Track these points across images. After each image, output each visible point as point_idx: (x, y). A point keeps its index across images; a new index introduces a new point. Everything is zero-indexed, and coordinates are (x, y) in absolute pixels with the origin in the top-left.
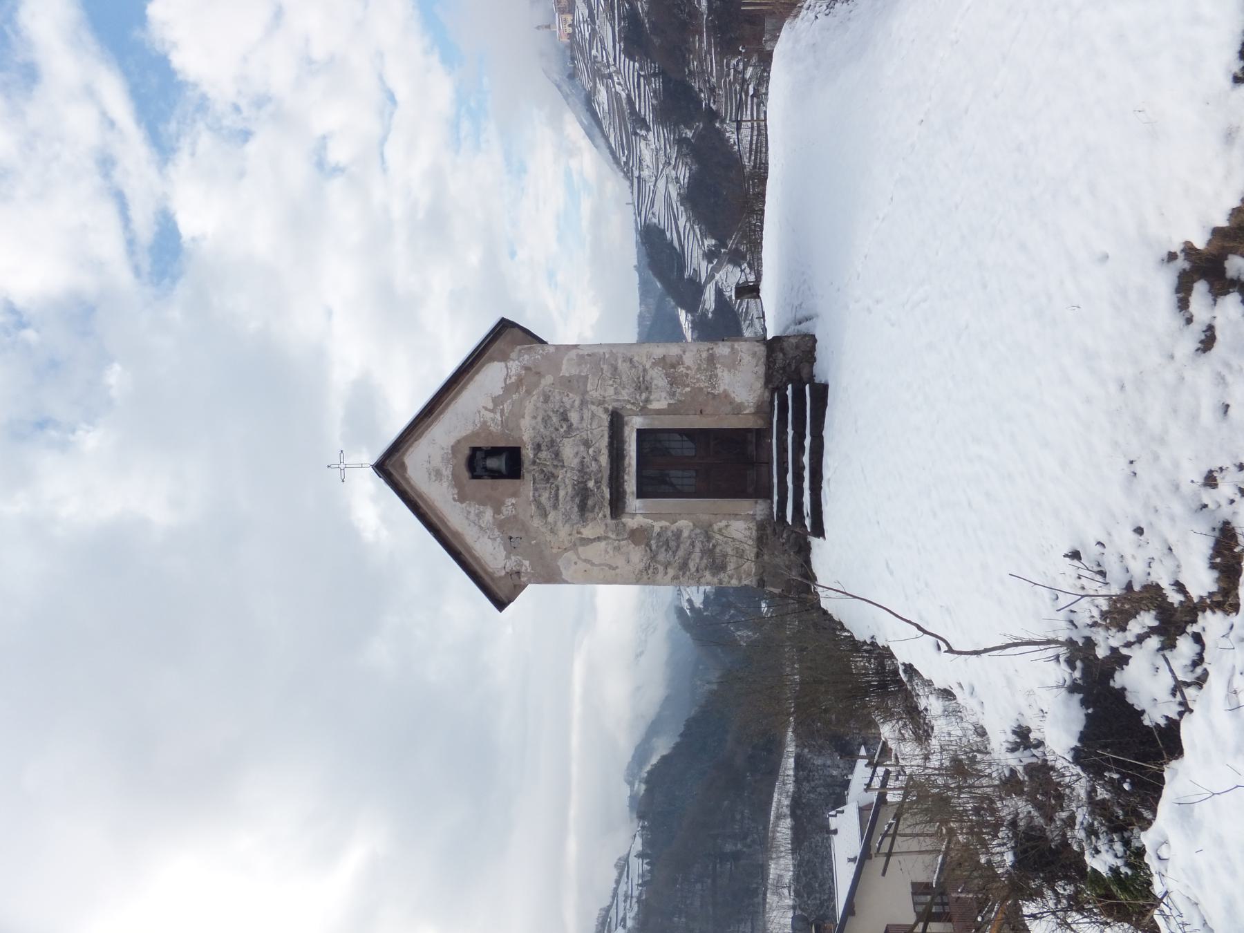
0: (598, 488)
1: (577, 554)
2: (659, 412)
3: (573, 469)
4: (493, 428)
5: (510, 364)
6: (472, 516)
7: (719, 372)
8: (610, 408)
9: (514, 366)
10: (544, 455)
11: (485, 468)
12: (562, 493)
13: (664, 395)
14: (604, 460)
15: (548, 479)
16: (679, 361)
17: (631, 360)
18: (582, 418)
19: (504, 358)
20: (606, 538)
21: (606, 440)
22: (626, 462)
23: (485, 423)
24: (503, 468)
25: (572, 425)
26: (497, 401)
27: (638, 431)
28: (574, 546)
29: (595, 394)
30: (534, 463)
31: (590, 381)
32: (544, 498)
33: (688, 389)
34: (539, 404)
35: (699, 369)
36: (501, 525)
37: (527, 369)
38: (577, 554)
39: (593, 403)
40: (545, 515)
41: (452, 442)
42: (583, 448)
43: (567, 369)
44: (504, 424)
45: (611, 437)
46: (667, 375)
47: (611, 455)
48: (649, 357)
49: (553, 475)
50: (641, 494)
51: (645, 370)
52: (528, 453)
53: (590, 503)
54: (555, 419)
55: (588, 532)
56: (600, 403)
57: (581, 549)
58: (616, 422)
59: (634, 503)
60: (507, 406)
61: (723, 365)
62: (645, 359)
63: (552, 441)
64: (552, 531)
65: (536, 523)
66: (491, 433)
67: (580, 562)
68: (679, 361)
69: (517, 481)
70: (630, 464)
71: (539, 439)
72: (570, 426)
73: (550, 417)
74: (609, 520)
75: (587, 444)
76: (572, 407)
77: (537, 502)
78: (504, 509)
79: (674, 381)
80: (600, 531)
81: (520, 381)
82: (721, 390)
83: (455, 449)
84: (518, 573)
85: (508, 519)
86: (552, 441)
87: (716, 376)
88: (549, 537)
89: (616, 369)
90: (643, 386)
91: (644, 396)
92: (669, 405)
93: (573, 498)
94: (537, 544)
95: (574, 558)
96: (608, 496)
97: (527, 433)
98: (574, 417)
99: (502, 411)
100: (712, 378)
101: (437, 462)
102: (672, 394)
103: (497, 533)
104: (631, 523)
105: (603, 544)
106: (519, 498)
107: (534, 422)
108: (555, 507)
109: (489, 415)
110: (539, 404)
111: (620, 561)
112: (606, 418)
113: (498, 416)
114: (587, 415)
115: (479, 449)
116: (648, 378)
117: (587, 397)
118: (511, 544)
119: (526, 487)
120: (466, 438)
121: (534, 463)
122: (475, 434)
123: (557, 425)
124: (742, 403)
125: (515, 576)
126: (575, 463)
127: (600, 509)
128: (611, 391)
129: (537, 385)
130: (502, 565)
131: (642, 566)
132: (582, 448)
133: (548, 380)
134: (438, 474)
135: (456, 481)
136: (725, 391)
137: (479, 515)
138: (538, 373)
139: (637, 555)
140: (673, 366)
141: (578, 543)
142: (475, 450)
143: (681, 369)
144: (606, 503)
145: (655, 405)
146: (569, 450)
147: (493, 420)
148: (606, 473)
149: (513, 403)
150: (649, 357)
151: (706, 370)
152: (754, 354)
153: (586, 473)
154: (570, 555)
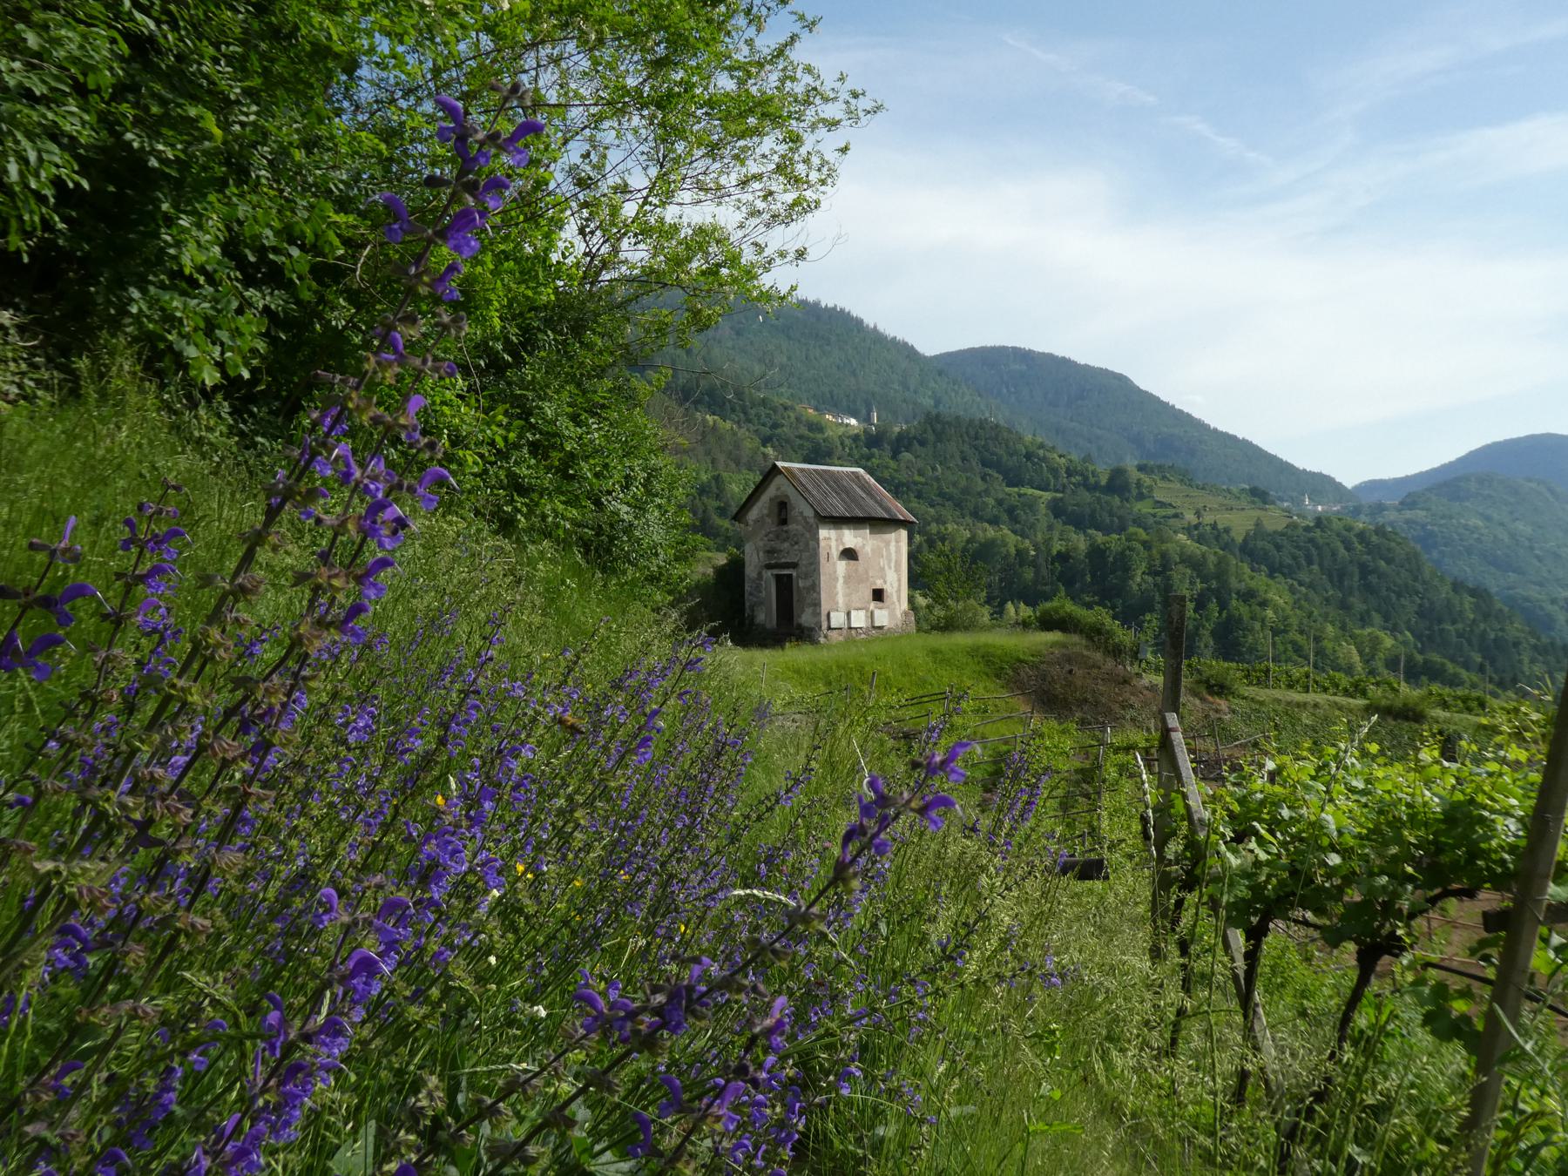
42: (789, 553)
43: (812, 543)
50: (778, 578)
58: (794, 566)
59: (768, 574)
90: (806, 576)
97: (792, 527)
106: (771, 525)
118: (757, 521)
146: (786, 545)
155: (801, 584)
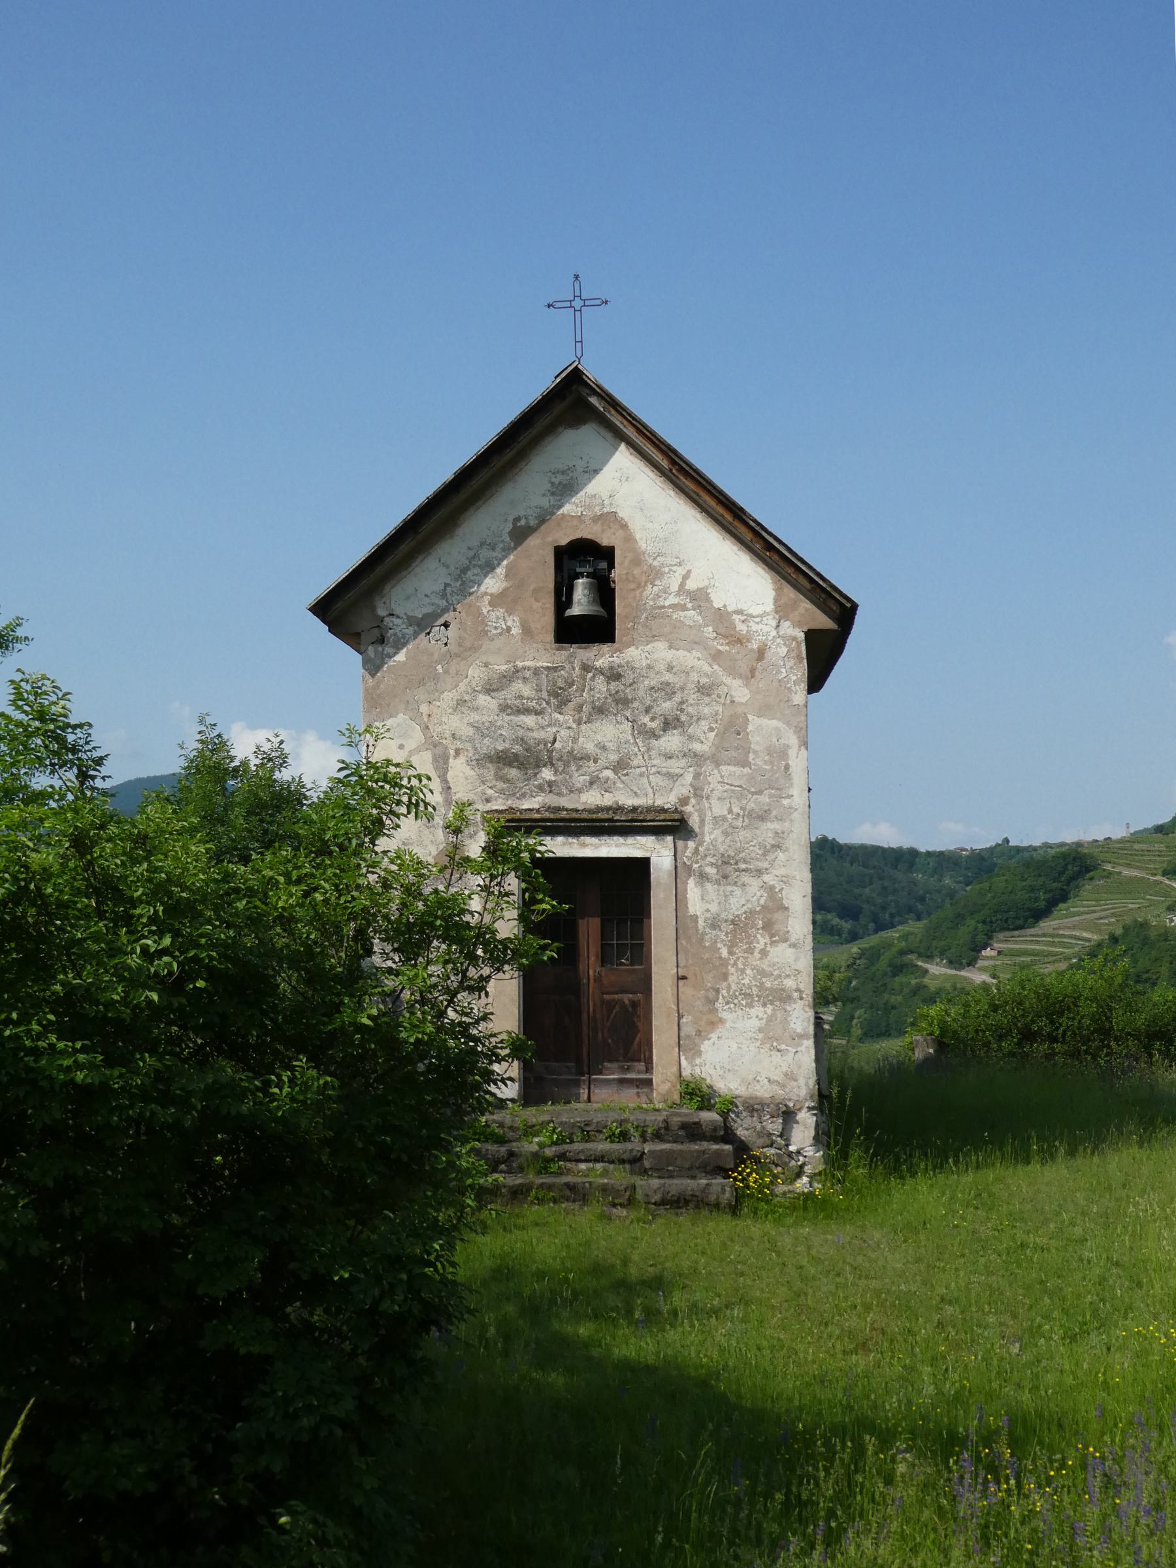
0: (541, 788)
1: (417, 750)
2: (679, 900)
3: (575, 740)
7: (758, 1010)
8: (688, 809)
10: (601, 685)
11: (578, 576)
12: (529, 720)
13: (714, 908)
14: (592, 799)
15: (556, 695)
16: (776, 935)
17: (777, 846)
19: (782, 611)
21: (628, 801)
22: (588, 840)
23: (655, 574)
24: (576, 610)
25: (657, 737)
26: (700, 598)
27: (645, 862)
29: (714, 778)
30: (586, 668)
31: (738, 770)
33: (724, 953)
34: (694, 677)
35: (763, 973)
37: (761, 654)
38: (417, 750)
39: (697, 776)
40: (489, 690)
44: (658, 614)
45: (634, 809)
46: (751, 914)
48: (786, 880)
51: (759, 872)
52: (602, 656)
53: (513, 773)
54: (666, 706)
56: (697, 791)
61: (770, 1019)
62: (782, 871)
63: (624, 702)
64: (461, 702)
65: (476, 674)
68: (776, 935)
69: (550, 637)
70: (584, 845)
71: (629, 677)
72: (653, 735)
75: (621, 766)
77: (514, 674)
78: (500, 612)
79: (740, 927)
81: (739, 640)
83: (610, 519)
84: (382, 640)
86: (624, 702)
87: (750, 1005)
88: (449, 697)
89: (762, 818)
90: (729, 868)
91: (710, 870)
92: (695, 918)
94: (436, 678)
96: (526, 805)
98: (672, 741)
99: (683, 608)
100: (747, 998)
102: (714, 925)
107: (661, 667)
108: (504, 708)
109: (675, 587)
110: (694, 677)
112: (668, 800)
113: (672, 600)
114: (675, 766)
115: (611, 566)
116: (745, 878)
117: (708, 767)
119: (543, 654)
120: (629, 539)
121: (586, 668)
122: (637, 559)
123: (657, 710)
124: (699, 1053)
125: (376, 632)
126: (588, 746)
127: (502, 792)
128: (719, 809)
129: (732, 672)
130: (398, 610)
132: (614, 757)
133: (741, 692)
136: (721, 1021)
138: (753, 671)
140: (768, 926)
141: (439, 750)
142: (607, 554)
143: (762, 941)
145: (693, 890)
146: (608, 733)
147: (666, 591)
148: (567, 802)
150: (786, 880)
151: (761, 987)
152: (790, 1076)
153: (567, 764)
155: (697, 900)
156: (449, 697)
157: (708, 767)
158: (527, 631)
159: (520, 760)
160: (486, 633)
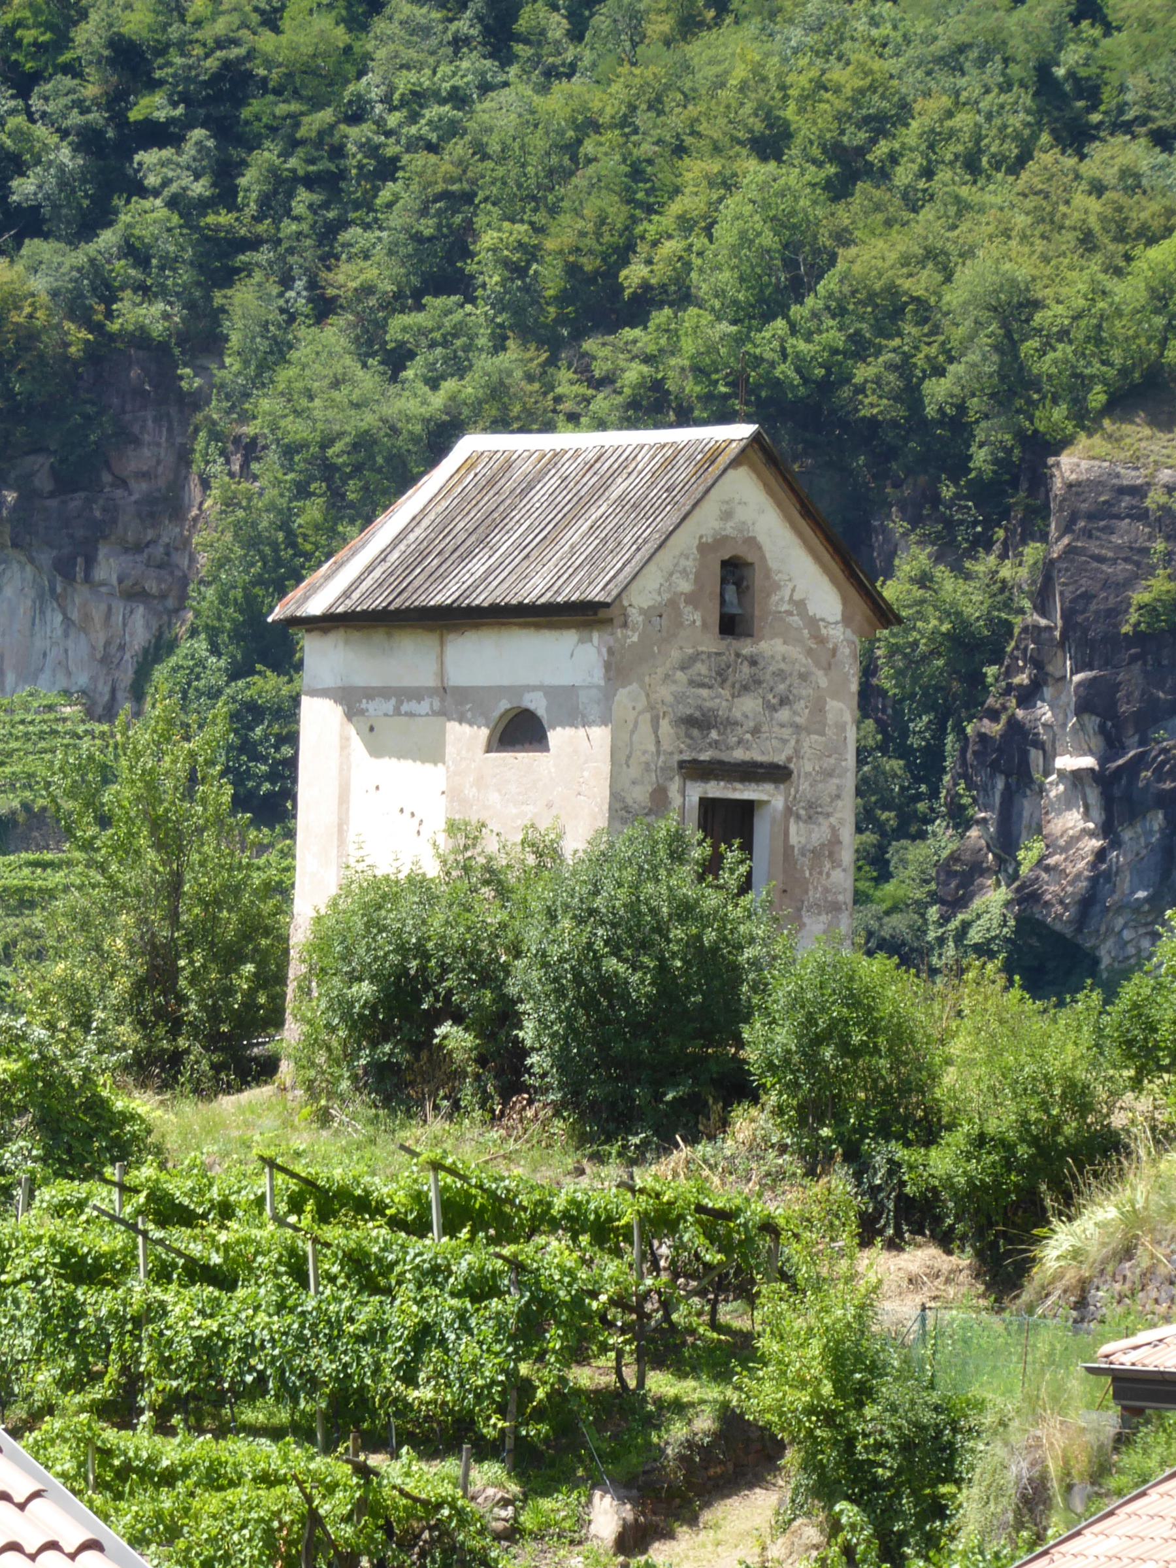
4: (774, 598)
5: (840, 627)
6: (683, 562)
9: (838, 634)
10: (746, 669)
12: (704, 692)
14: (739, 755)
17: (838, 797)
18: (782, 726)
19: (847, 620)
20: (658, 753)
21: (760, 758)
22: (738, 786)
26: (801, 605)
28: (651, 707)
29: (806, 745)
30: (738, 655)
32: (701, 668)
36: (672, 603)
37: (834, 652)
40: (683, 668)
41: (761, 539)
45: (761, 765)
46: (822, 845)
47: (744, 764)
49: (724, 681)
51: (828, 815)
53: (695, 732)
55: (665, 726)
57: (648, 716)
58: (778, 774)
60: (795, 620)
63: (759, 682)
64: (667, 676)
65: (675, 655)
66: (768, 596)
67: (634, 714)
71: (762, 664)
72: (774, 709)
73: (784, 680)
74: (677, 757)
75: (756, 731)
76: (795, 713)
78: (690, 608)
80: (666, 746)
81: (821, 640)
82: (806, 920)
85: (679, 614)
86: (759, 682)
88: (660, 671)
90: (813, 812)
93: (700, 708)
95: (640, 707)
97: (770, 647)
98: (784, 714)
101: (741, 514)
103: (666, 596)
104: (674, 788)
105: (653, 749)
108: (692, 683)
111: (634, 771)
112: (780, 759)
113: (785, 607)
116: (821, 819)
117: (803, 735)
119: (711, 643)
120: (763, 558)
126: (737, 714)
128: (808, 767)
129: (817, 664)
131: (629, 801)
134: (727, 515)
135: (721, 541)
137: (684, 572)
139: (640, 795)
143: (828, 865)
144: (694, 755)
146: (749, 706)
148: (725, 757)
149: (798, 629)
150: (841, 822)
154: (642, 703)
156: (660, 671)
157: (803, 735)
158: (705, 625)
159: (697, 723)
160: (681, 624)
